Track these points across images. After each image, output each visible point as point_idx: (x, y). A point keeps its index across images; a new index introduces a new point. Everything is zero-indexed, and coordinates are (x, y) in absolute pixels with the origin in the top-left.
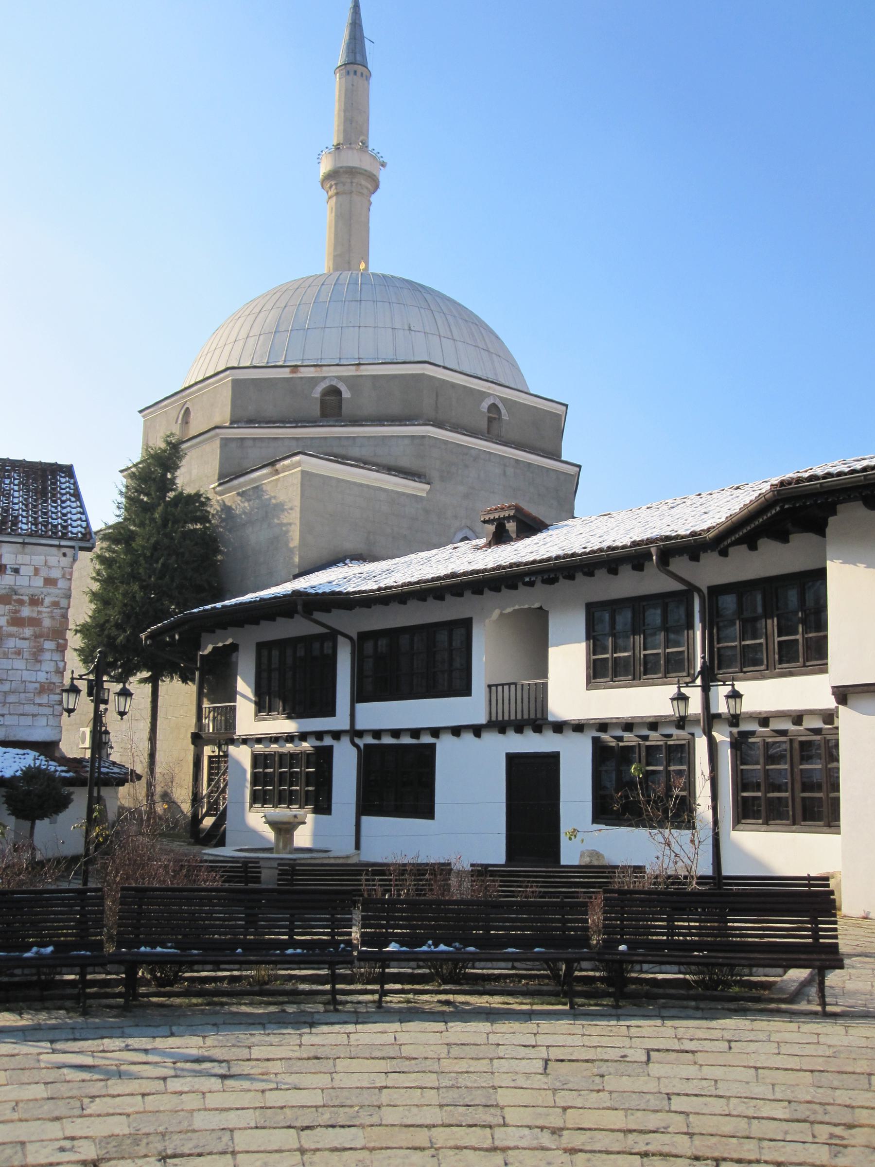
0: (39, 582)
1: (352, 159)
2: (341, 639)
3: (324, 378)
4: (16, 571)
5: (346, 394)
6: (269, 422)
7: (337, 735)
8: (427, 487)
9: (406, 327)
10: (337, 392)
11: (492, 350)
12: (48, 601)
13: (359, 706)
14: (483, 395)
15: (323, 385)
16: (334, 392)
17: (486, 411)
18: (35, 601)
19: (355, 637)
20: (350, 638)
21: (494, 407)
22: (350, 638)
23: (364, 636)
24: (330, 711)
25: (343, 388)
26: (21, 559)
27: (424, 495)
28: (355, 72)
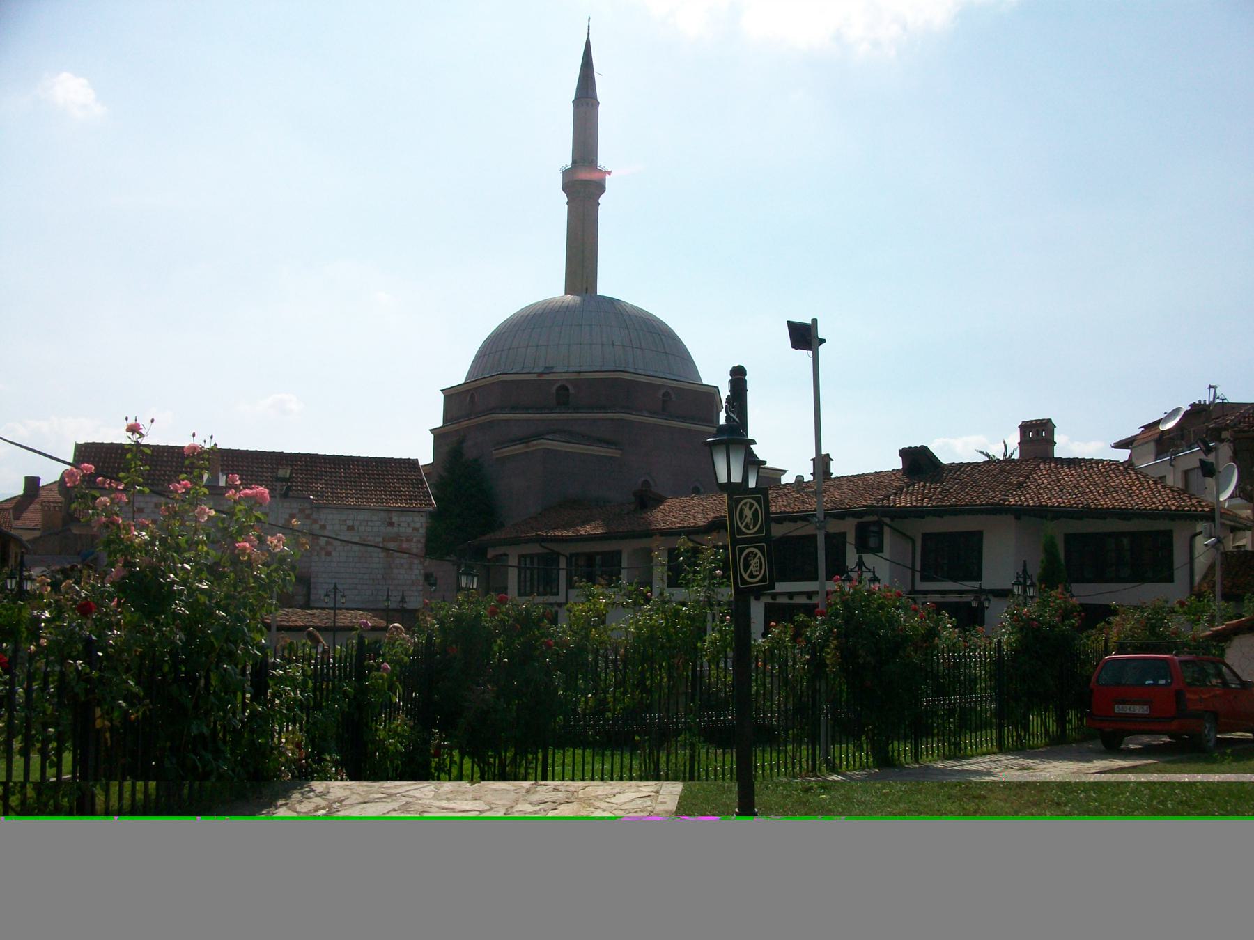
0: (410, 530)
1: (584, 175)
2: (561, 557)
3: (557, 381)
4: (399, 525)
5: (572, 391)
6: (526, 409)
7: (560, 605)
8: (620, 452)
9: (611, 343)
10: (567, 389)
11: (668, 352)
12: (414, 540)
13: (571, 591)
14: (659, 387)
15: (558, 385)
16: (563, 388)
17: (661, 397)
18: (409, 540)
19: (568, 555)
20: (566, 556)
21: (666, 394)
22: (566, 556)
23: (572, 555)
24: (557, 594)
25: (570, 387)
26: (403, 519)
27: (618, 456)
28: (587, 104)
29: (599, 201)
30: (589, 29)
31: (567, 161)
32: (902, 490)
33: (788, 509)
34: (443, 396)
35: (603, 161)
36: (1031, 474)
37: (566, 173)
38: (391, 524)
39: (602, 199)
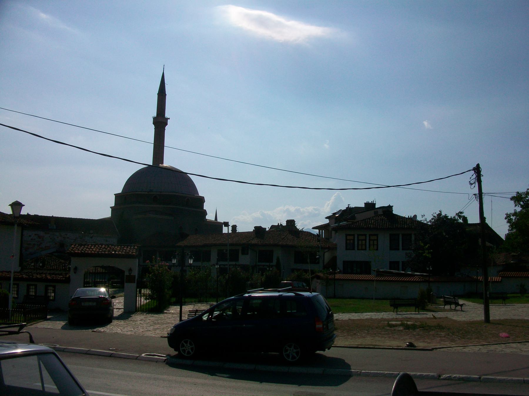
29: (165, 128)
30: (164, 69)
31: (155, 114)
32: (254, 238)
33: (224, 243)
34: (115, 196)
35: (167, 116)
36: (287, 235)
37: (154, 118)
38: (107, 241)
39: (166, 128)
